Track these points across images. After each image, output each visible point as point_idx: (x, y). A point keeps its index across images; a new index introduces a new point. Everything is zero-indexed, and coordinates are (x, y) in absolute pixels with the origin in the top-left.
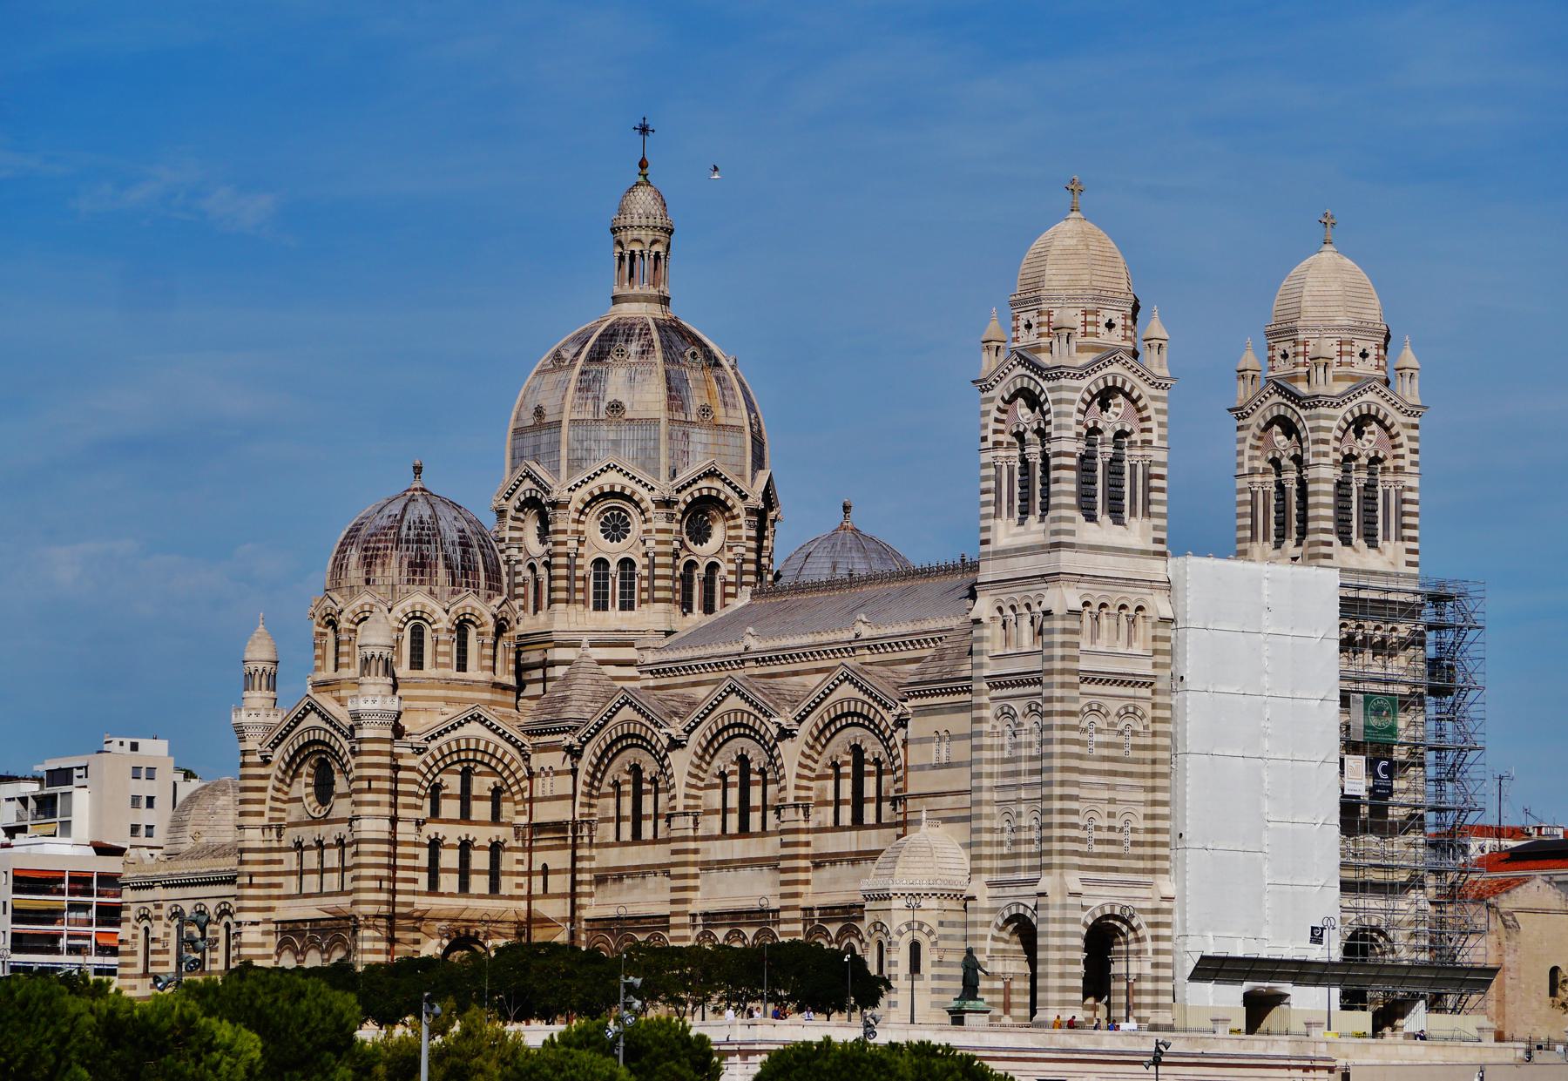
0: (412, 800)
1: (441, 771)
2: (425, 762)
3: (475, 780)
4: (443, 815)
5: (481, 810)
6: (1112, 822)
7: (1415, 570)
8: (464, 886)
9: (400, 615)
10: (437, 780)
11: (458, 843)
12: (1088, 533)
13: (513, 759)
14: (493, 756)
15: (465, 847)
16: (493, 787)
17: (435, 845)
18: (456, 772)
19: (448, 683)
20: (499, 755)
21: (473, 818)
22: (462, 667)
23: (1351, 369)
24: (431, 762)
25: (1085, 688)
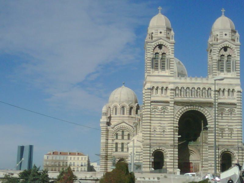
0: (111, 136)
1: (117, 131)
2: (114, 130)
3: (125, 132)
4: (119, 138)
5: (126, 137)
6: (160, 130)
7: (239, 77)
8: (122, 150)
9: (113, 106)
10: (117, 133)
11: (121, 143)
12: (156, 73)
13: (131, 129)
14: (127, 128)
15: (122, 144)
16: (128, 133)
17: (117, 144)
18: (121, 131)
19: (120, 117)
20: (128, 128)
21: (124, 139)
22: (123, 114)
23: (222, 37)
24: (115, 130)
25: (152, 104)
